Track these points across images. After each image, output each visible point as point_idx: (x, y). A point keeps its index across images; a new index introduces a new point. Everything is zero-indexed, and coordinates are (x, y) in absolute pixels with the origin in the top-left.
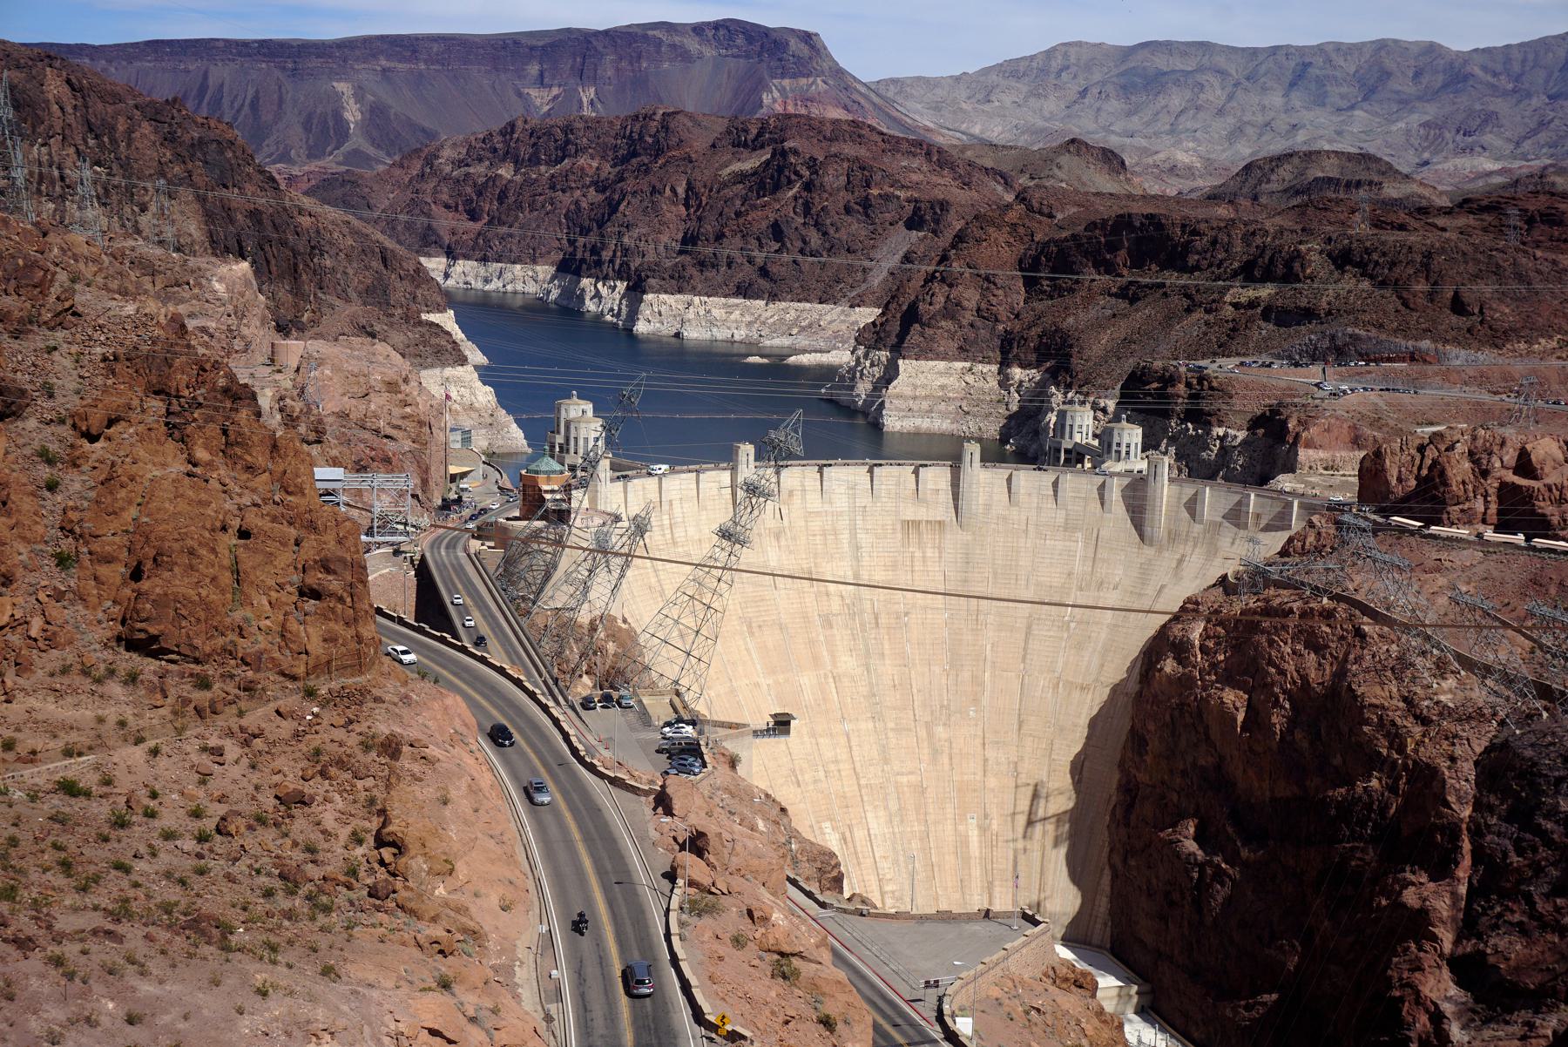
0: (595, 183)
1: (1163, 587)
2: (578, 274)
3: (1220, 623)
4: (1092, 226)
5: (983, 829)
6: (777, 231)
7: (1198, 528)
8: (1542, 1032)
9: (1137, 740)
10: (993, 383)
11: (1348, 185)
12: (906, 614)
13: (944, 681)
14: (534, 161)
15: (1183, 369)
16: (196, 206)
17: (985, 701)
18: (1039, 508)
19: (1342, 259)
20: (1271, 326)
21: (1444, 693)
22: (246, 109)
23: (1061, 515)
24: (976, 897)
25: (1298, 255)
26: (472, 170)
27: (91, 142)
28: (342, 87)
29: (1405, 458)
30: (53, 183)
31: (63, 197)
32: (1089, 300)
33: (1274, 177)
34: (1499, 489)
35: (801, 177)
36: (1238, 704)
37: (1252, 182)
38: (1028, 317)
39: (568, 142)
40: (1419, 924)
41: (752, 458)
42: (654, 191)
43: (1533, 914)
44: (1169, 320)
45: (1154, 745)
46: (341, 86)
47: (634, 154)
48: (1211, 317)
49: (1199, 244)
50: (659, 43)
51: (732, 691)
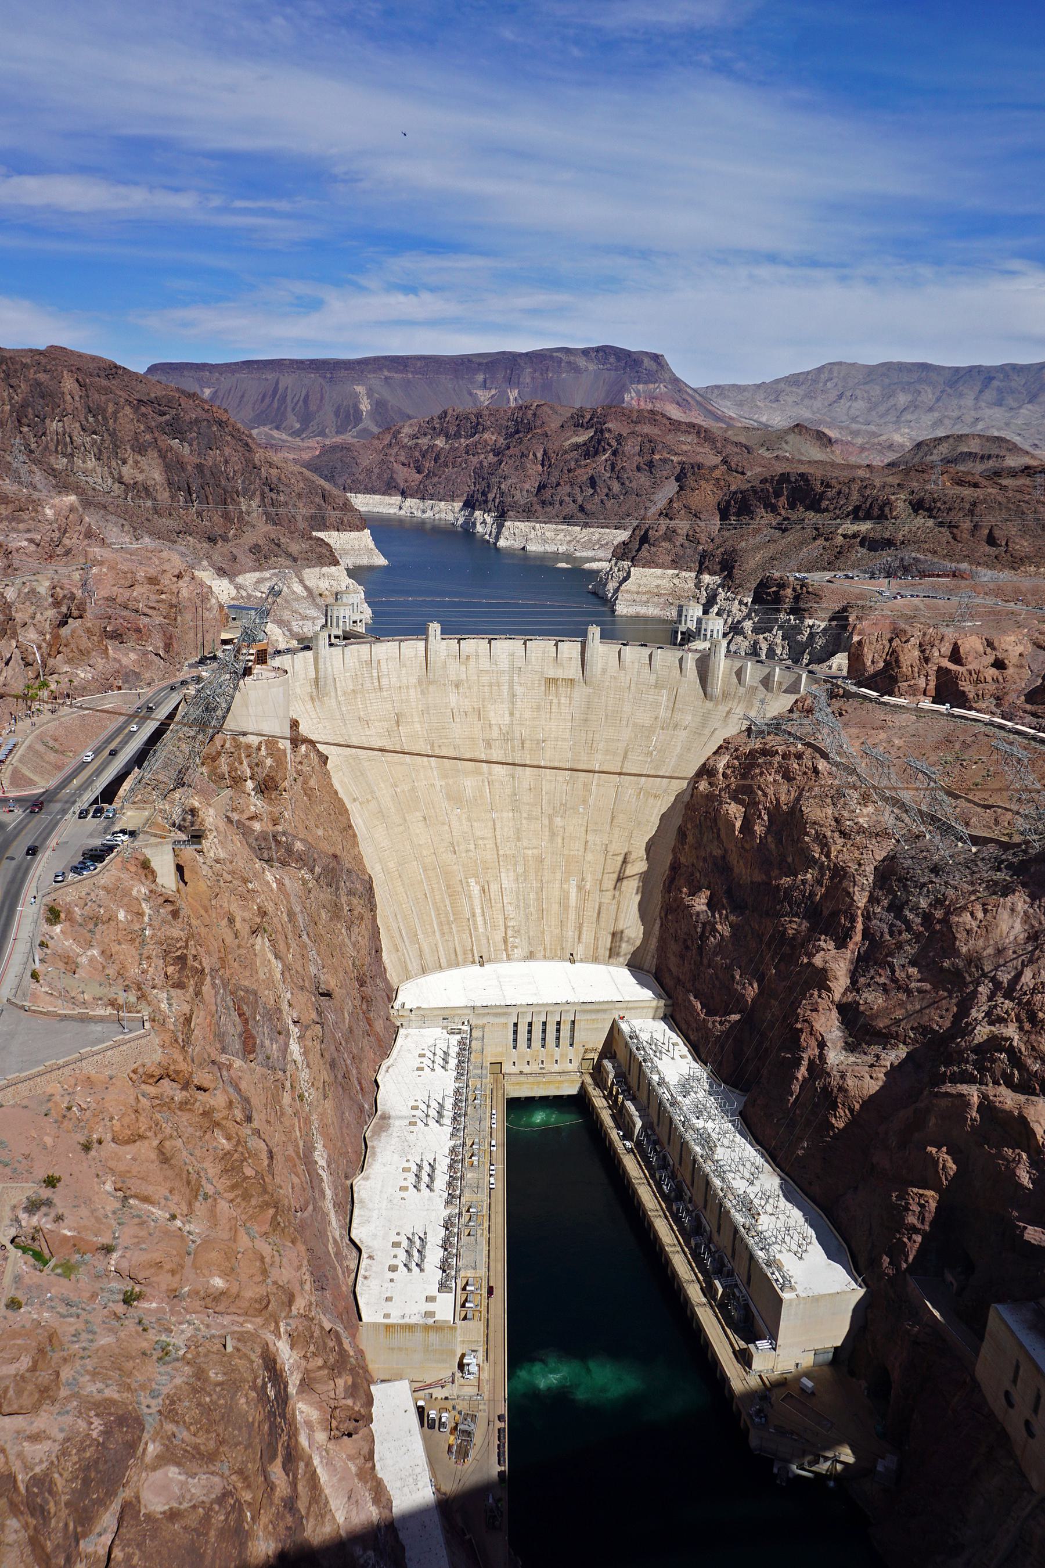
0: (493, 450)
1: (715, 729)
2: (474, 509)
3: (737, 758)
4: (764, 481)
5: (580, 888)
6: (593, 482)
7: (742, 690)
8: (883, 1063)
9: (682, 833)
10: (691, 585)
11: (982, 457)
12: (544, 741)
13: (564, 787)
14: (457, 435)
15: (791, 579)
16: (160, 461)
17: (591, 802)
18: (639, 672)
19: (917, 506)
20: (865, 551)
21: (864, 816)
22: (301, 402)
23: (653, 677)
24: (570, 933)
25: (888, 503)
26: (420, 441)
27: (91, 419)
28: (360, 389)
29: (879, 646)
30: (65, 445)
31: (72, 455)
32: (758, 530)
33: (935, 452)
34: (937, 671)
35: (612, 447)
36: (737, 815)
37: (921, 454)
38: (718, 541)
39: (478, 424)
40: (821, 979)
41: (439, 632)
42: (523, 455)
43: (894, 980)
44: (803, 543)
45: (690, 839)
46: (360, 389)
47: (517, 432)
48: (827, 544)
49: (830, 493)
50: (560, 361)
51: (413, 789)
